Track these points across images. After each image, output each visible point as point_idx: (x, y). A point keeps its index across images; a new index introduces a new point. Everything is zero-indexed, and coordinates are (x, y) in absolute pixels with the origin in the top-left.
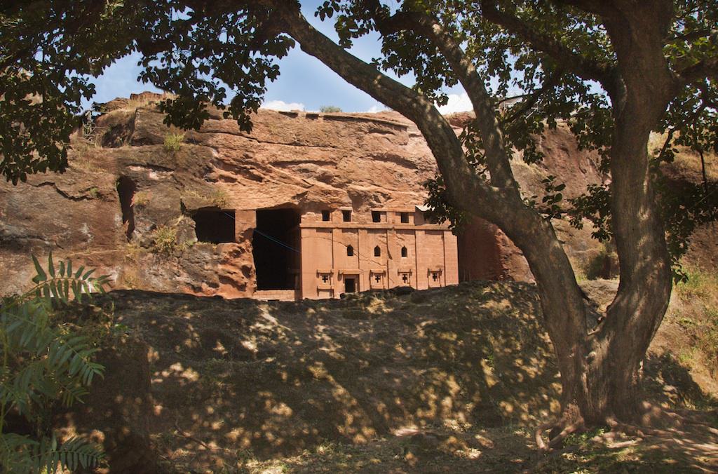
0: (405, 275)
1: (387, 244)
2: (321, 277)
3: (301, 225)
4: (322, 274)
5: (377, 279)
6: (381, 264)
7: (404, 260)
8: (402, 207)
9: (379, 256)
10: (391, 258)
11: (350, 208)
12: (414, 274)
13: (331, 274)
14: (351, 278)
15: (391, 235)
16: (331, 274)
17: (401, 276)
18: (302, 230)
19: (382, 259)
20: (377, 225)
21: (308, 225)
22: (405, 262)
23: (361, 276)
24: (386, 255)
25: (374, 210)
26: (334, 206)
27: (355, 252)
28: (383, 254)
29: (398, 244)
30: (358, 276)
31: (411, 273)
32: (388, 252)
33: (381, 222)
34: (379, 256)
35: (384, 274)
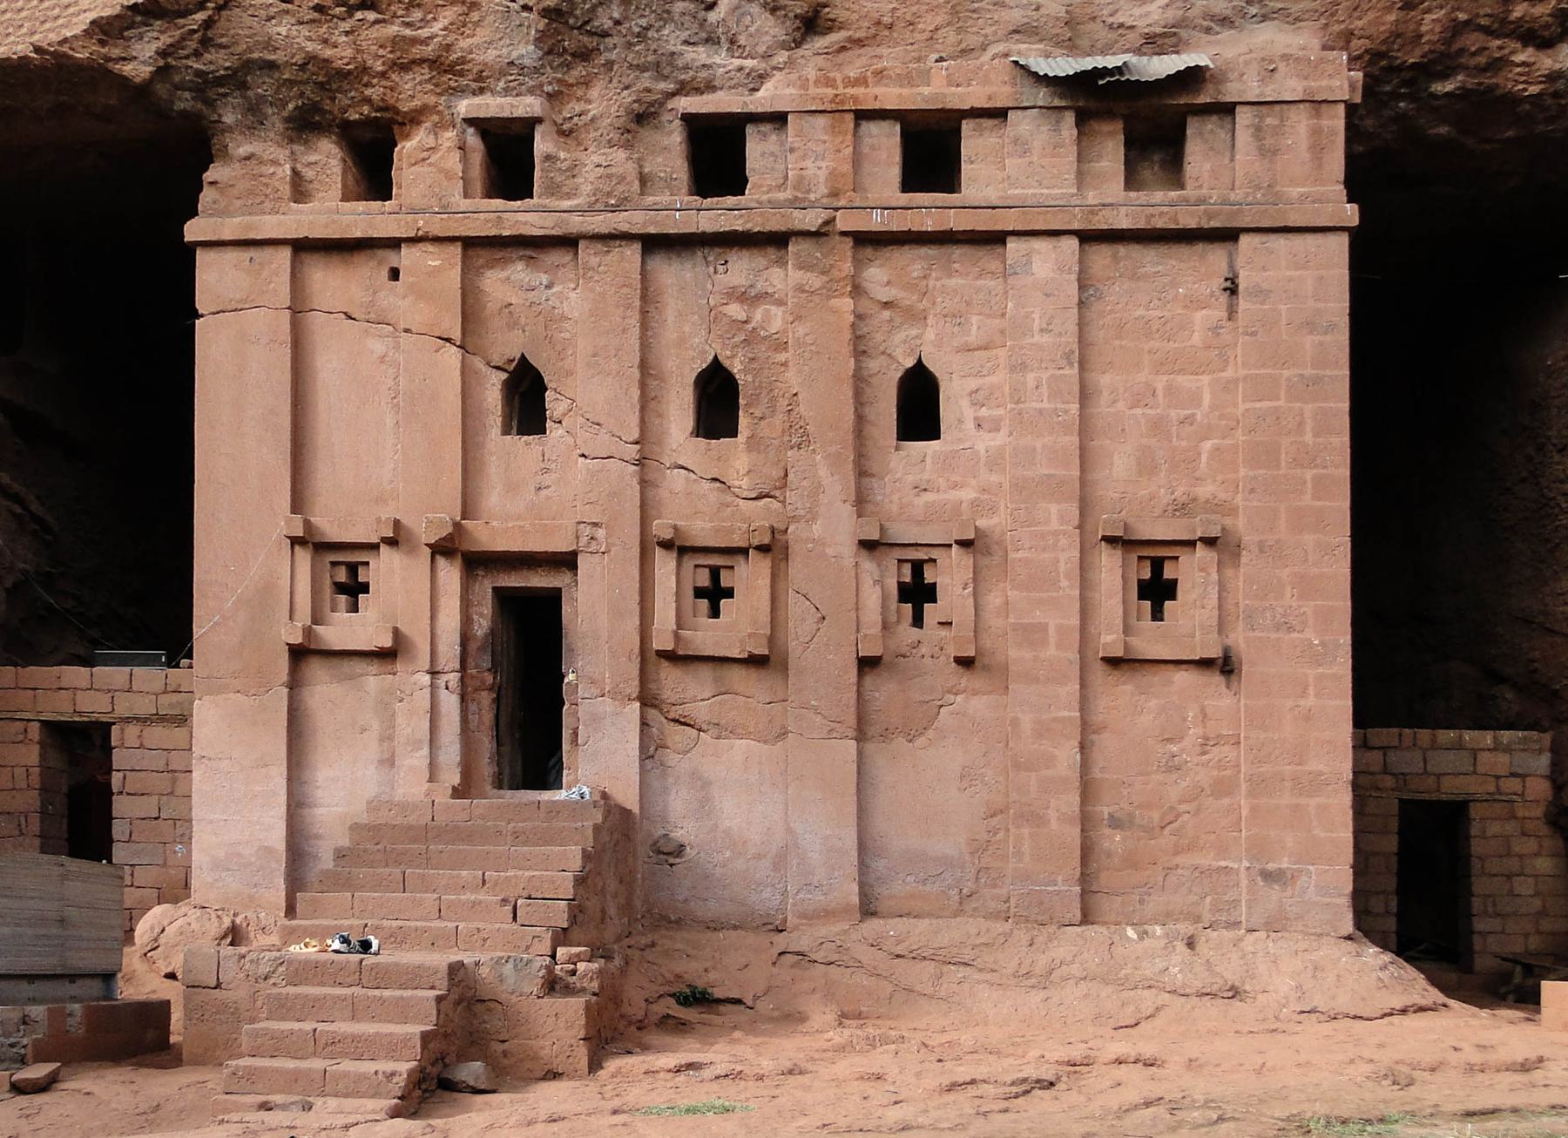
3: (193, 231)
6: (743, 484)
8: (907, 79)
11: (527, 105)
15: (815, 281)
18: (201, 257)
20: (716, 215)
21: (230, 228)
26: (411, 90)
27: (554, 404)
33: (750, 195)
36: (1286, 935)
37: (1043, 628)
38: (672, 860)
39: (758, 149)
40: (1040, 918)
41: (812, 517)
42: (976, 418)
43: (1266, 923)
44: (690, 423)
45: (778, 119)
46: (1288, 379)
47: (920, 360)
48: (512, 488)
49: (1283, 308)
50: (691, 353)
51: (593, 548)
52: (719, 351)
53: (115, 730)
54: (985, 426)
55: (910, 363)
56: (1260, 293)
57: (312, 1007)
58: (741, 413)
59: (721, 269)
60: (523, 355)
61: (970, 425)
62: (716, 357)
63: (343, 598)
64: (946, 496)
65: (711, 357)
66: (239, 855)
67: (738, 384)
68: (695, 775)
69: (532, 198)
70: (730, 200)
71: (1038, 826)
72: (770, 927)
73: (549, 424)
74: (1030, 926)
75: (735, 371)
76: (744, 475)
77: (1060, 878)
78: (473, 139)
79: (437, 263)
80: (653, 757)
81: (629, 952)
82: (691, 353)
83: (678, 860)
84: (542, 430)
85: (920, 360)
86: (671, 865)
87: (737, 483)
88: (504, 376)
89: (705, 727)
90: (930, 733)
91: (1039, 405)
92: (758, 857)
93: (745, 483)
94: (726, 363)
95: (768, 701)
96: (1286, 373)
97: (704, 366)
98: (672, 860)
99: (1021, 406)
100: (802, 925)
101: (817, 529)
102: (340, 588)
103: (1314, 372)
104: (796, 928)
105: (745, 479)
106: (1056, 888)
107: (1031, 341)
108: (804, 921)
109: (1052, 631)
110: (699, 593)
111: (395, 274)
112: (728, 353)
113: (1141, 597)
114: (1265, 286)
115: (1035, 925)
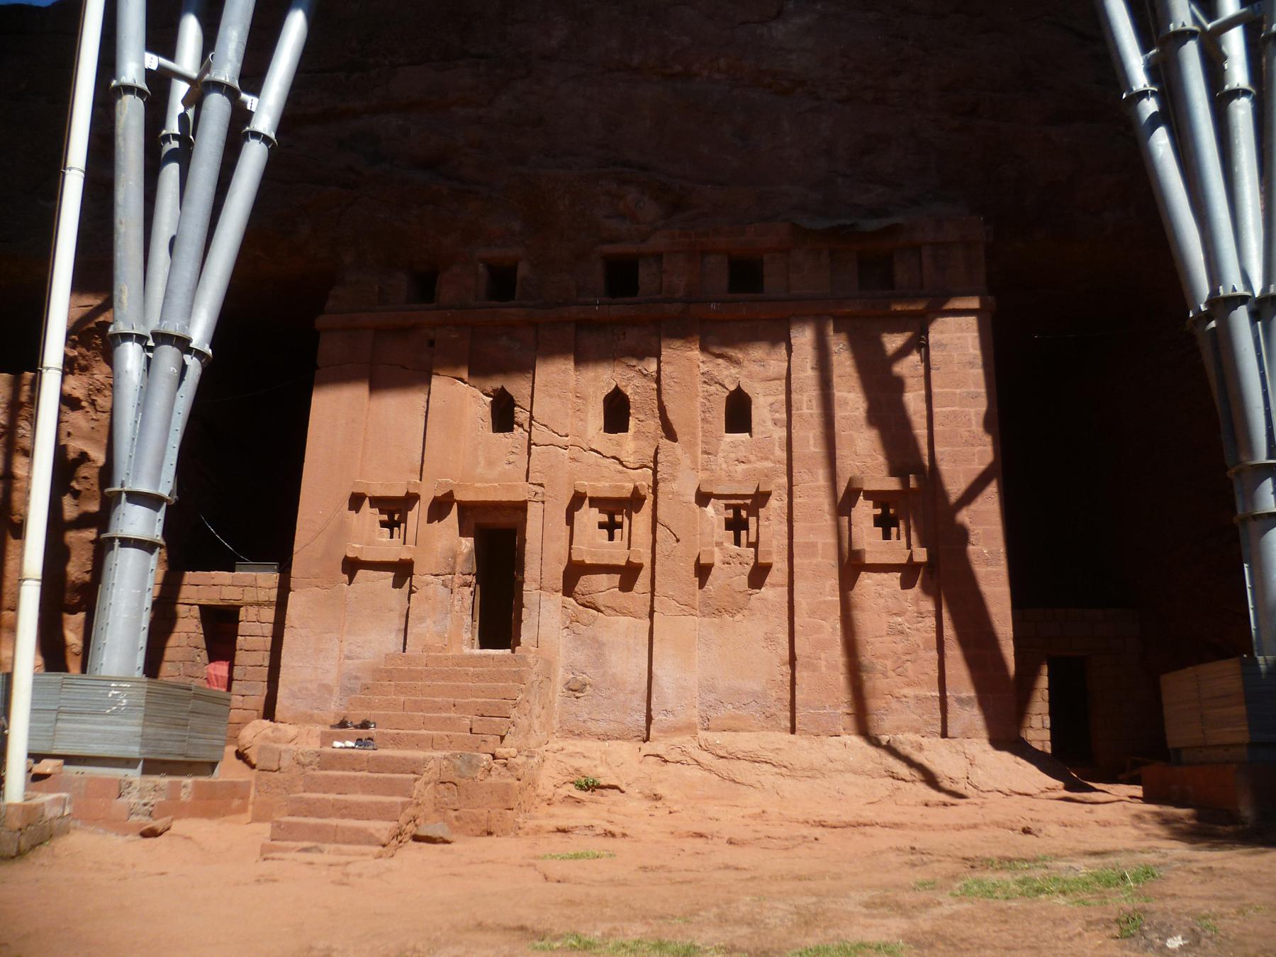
0: (737, 509)
1: (658, 381)
2: (370, 516)
3: (321, 321)
4: (377, 502)
5: (610, 527)
6: (630, 459)
7: (734, 445)
9: (626, 430)
10: (670, 434)
12: (776, 504)
13: (411, 499)
14: (502, 520)
16: (411, 499)
17: (715, 514)
19: (629, 444)
22: (741, 455)
23: (534, 512)
24: (654, 424)
25: (608, 249)
27: (521, 415)
28: (642, 421)
29: (710, 380)
30: (520, 508)
31: (761, 498)
32: (662, 409)
34: (626, 430)
35: (634, 502)
36: (975, 740)
37: (814, 545)
38: (577, 694)
39: (645, 275)
40: (815, 731)
41: (674, 478)
42: (773, 419)
43: (963, 733)
44: (601, 423)
45: (658, 256)
46: (960, 394)
47: (739, 387)
48: (490, 463)
49: (955, 355)
50: (602, 384)
51: (539, 498)
52: (618, 383)
53: (242, 610)
54: (779, 424)
55: (732, 388)
56: (942, 346)
57: (339, 786)
58: (631, 418)
59: (622, 337)
60: (502, 386)
61: (769, 424)
62: (617, 386)
63: (387, 530)
64: (755, 465)
65: (614, 386)
66: (306, 689)
67: (628, 399)
68: (595, 639)
69: (514, 299)
70: (628, 299)
71: (813, 671)
72: (639, 738)
73: (515, 426)
74: (808, 736)
75: (628, 394)
76: (631, 454)
77: (827, 706)
78: (481, 268)
79: (456, 336)
80: (568, 628)
81: (546, 753)
82: (602, 384)
83: (582, 695)
84: (511, 430)
85: (739, 387)
86: (577, 698)
87: (627, 459)
88: (492, 399)
89: (603, 609)
90: (746, 612)
91: (811, 411)
92: (633, 692)
93: (631, 459)
94: (623, 389)
95: (642, 592)
96: (958, 391)
97: (609, 391)
98: (577, 694)
99: (799, 412)
100: (660, 737)
101: (675, 486)
102: (383, 524)
103: (976, 390)
104: (655, 739)
105: (632, 456)
106: (825, 711)
107: (805, 374)
108: (662, 734)
109: (820, 547)
110: (601, 526)
111: (432, 343)
112: (624, 384)
113: (876, 525)
114: (944, 342)
115: (812, 736)
